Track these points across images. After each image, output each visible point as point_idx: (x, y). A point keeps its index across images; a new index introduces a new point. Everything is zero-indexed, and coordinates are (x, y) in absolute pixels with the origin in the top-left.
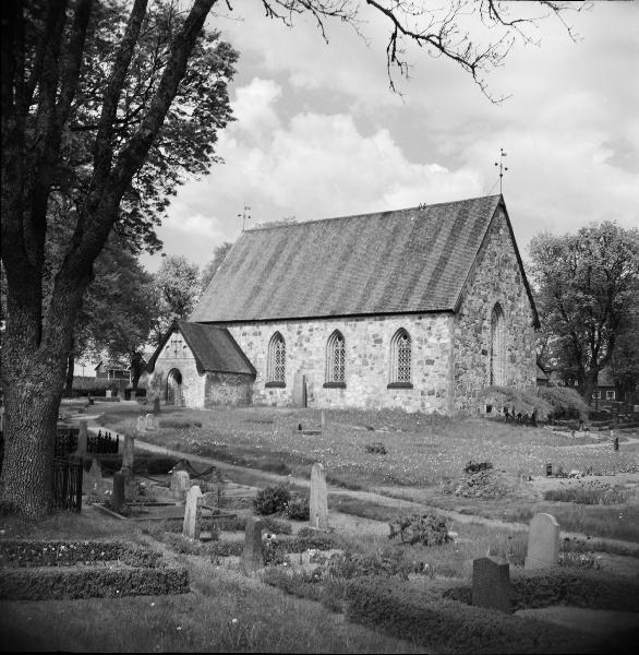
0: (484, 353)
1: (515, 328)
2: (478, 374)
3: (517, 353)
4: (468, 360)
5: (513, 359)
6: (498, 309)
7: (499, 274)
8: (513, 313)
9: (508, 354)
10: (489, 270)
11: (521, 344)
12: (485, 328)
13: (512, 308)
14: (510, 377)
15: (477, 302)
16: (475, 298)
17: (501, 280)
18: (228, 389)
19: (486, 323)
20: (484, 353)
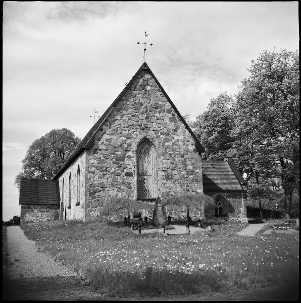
0: (129, 175)
1: (171, 155)
2: (119, 190)
3: (175, 172)
4: (108, 180)
5: (168, 177)
6: (145, 144)
7: (147, 118)
8: (167, 144)
9: (161, 174)
10: (134, 116)
11: (180, 166)
12: (129, 157)
13: (166, 140)
14: (165, 190)
15: (117, 140)
16: (114, 137)
17: (150, 121)
18: (40, 214)
19: (130, 153)
20: (129, 175)
